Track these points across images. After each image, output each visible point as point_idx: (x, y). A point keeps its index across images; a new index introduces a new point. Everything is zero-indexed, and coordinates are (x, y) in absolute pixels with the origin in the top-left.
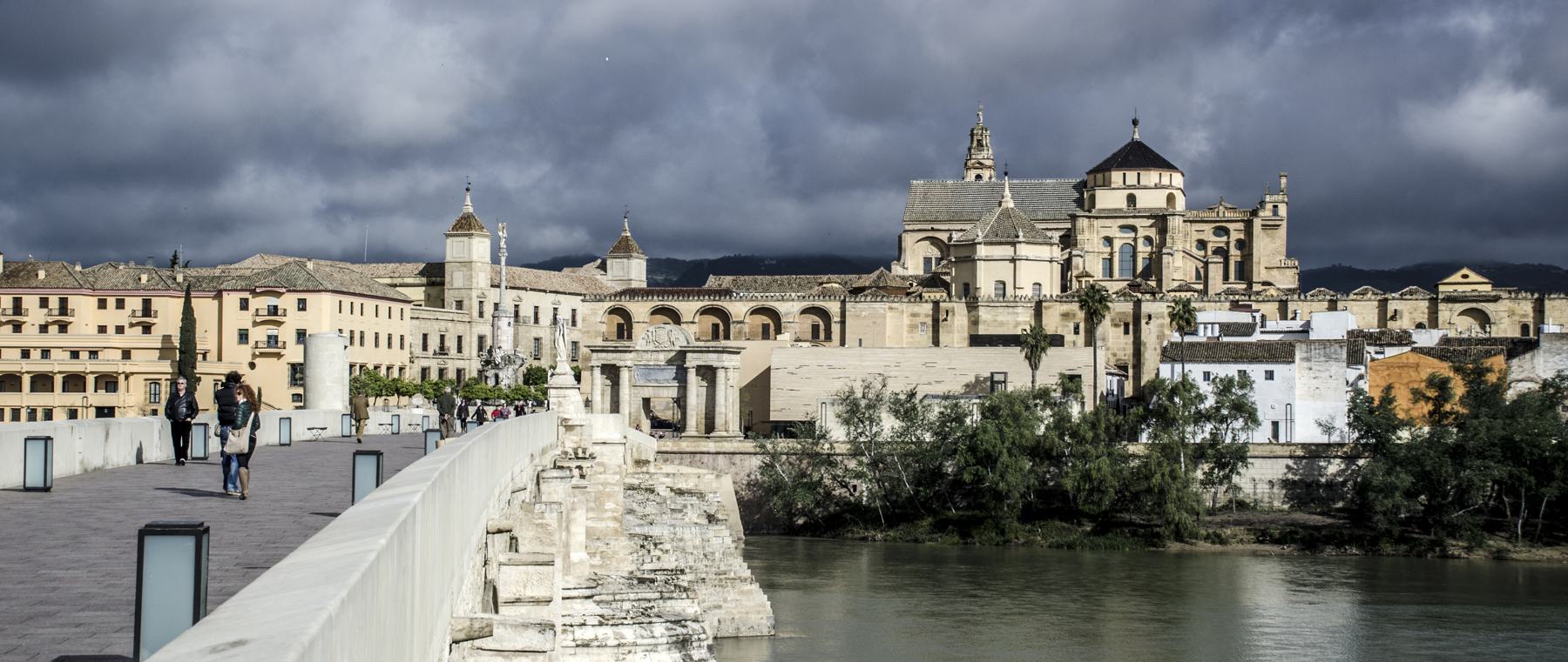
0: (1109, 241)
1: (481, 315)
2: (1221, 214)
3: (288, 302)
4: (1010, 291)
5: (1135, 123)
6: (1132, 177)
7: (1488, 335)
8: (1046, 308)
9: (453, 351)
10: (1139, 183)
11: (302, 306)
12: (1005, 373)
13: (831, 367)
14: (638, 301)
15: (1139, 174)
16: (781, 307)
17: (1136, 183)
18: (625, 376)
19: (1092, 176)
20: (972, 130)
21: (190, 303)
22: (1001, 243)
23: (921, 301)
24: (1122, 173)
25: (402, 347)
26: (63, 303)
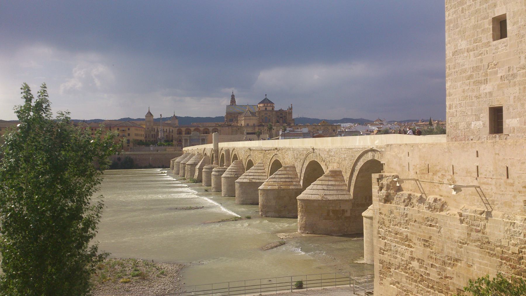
0: (263, 116)
1: (152, 131)
3: (127, 129)
4: (249, 125)
5: (266, 95)
9: (148, 137)
11: (129, 129)
13: (222, 139)
16: (209, 128)
18: (188, 141)
25: (143, 136)
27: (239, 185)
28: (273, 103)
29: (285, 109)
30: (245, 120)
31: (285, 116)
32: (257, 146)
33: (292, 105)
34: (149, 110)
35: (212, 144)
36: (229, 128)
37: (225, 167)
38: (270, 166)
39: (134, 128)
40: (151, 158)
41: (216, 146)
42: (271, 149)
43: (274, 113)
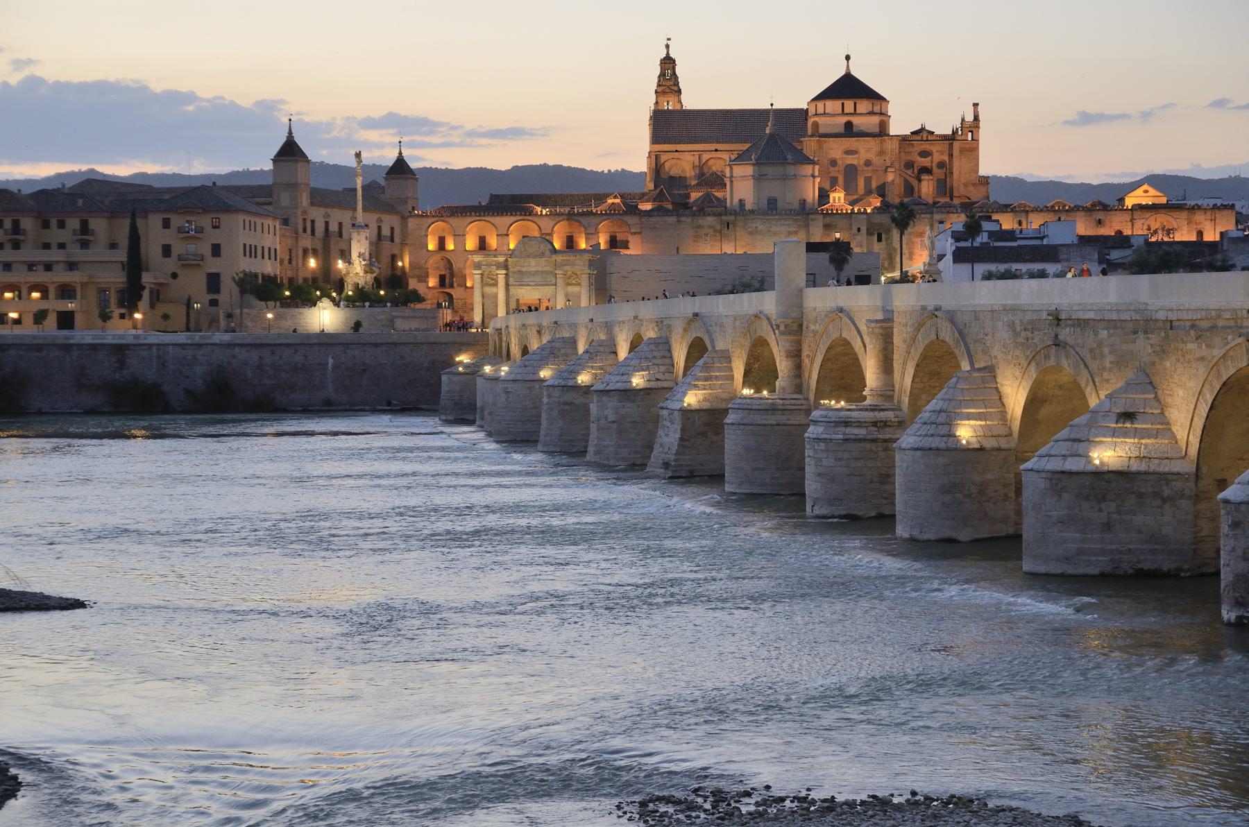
2: (925, 139)
3: (205, 221)
4: (780, 204)
5: (848, 58)
6: (849, 106)
7: (1172, 240)
8: (812, 220)
10: (855, 110)
12: (814, 274)
14: (458, 216)
15: (855, 104)
17: (852, 111)
19: (814, 104)
20: (661, 60)
21: (135, 221)
22: (773, 164)
23: (705, 215)
24: (838, 103)
25: (276, 259)
26: (16, 224)
27: (1042, 484)
28: (881, 99)
29: (943, 128)
30: (758, 178)
31: (941, 165)
32: (1109, 304)
33: (976, 105)
34: (290, 133)
35: (772, 292)
36: (679, 221)
37: (867, 402)
38: (1209, 397)
39: (241, 217)
40: (331, 361)
41: (797, 301)
42: (1213, 314)
43: (891, 146)
